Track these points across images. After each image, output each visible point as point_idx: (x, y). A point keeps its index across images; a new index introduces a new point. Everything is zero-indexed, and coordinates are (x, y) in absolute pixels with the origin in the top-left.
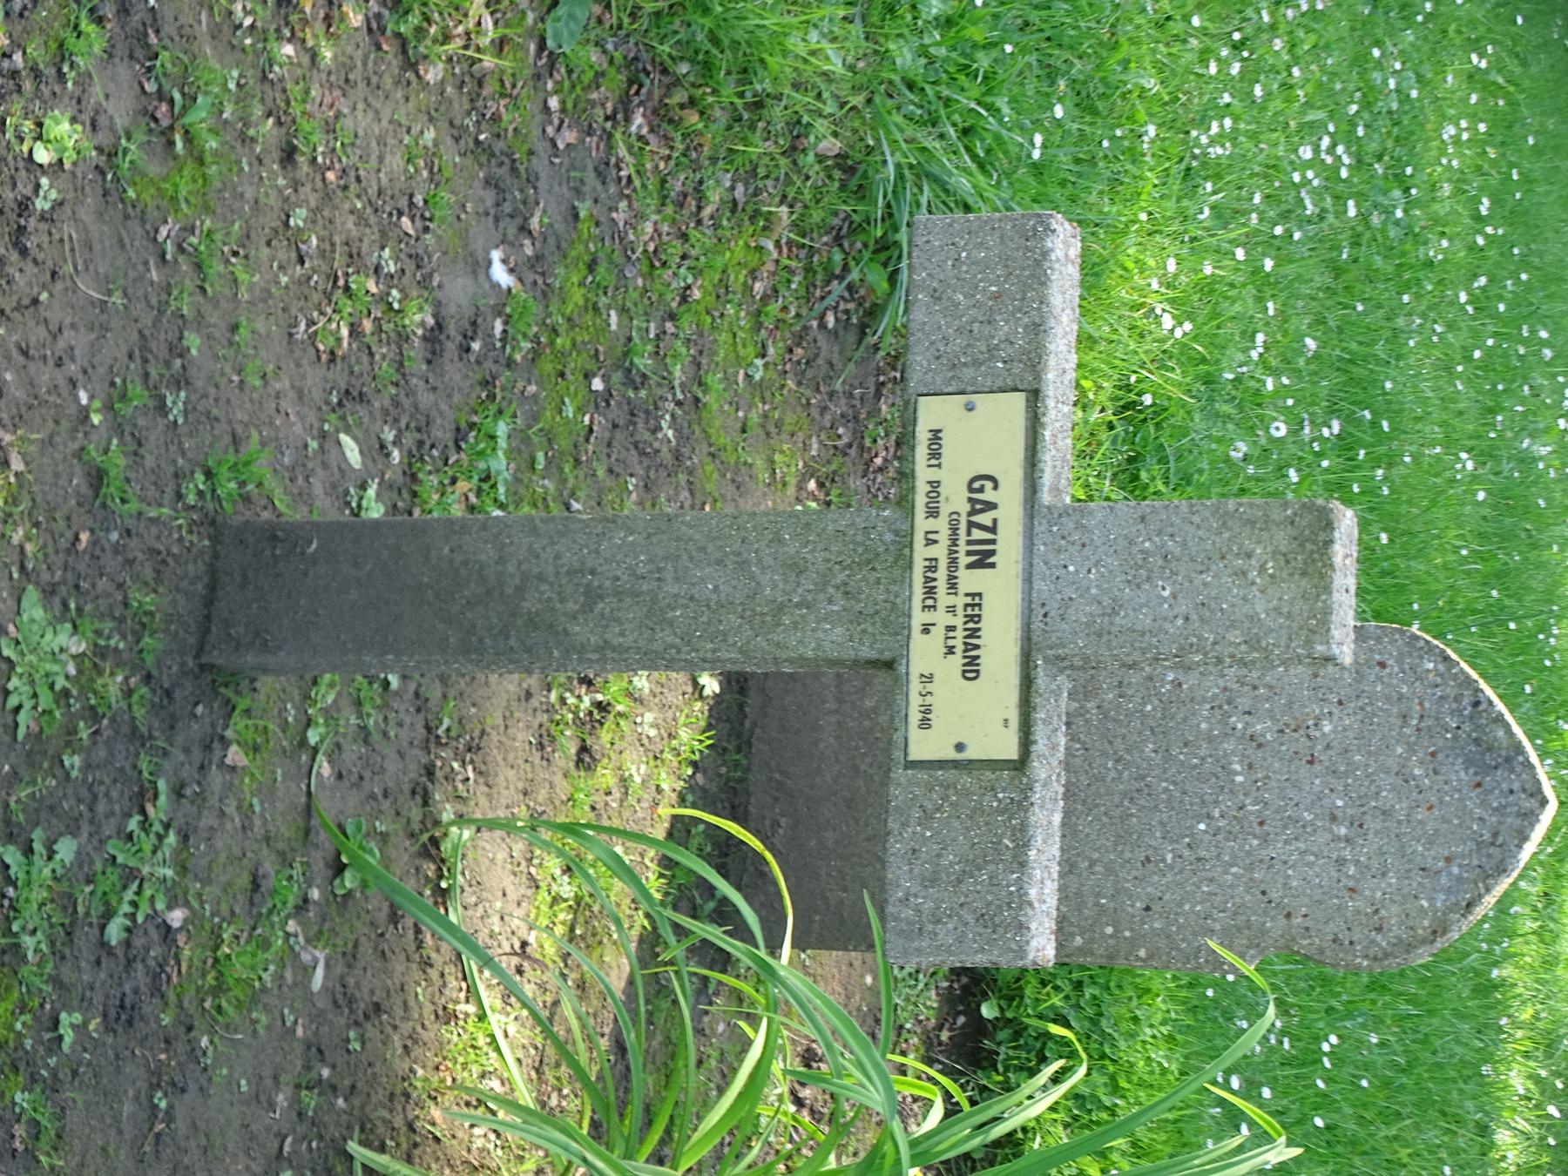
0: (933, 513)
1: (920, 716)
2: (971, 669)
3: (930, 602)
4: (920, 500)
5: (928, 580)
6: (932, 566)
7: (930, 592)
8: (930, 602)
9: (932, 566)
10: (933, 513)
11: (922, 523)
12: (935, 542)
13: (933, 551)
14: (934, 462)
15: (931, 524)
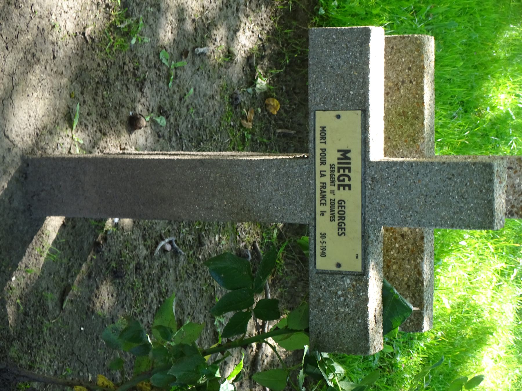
0: (323, 163)
1: (321, 251)
2: (342, 230)
3: (323, 202)
4: (318, 157)
5: (322, 192)
6: (324, 186)
7: (323, 197)
8: (323, 202)
9: (324, 186)
10: (323, 163)
11: (319, 168)
12: (325, 175)
13: (324, 179)
14: (322, 141)
15: (323, 168)
